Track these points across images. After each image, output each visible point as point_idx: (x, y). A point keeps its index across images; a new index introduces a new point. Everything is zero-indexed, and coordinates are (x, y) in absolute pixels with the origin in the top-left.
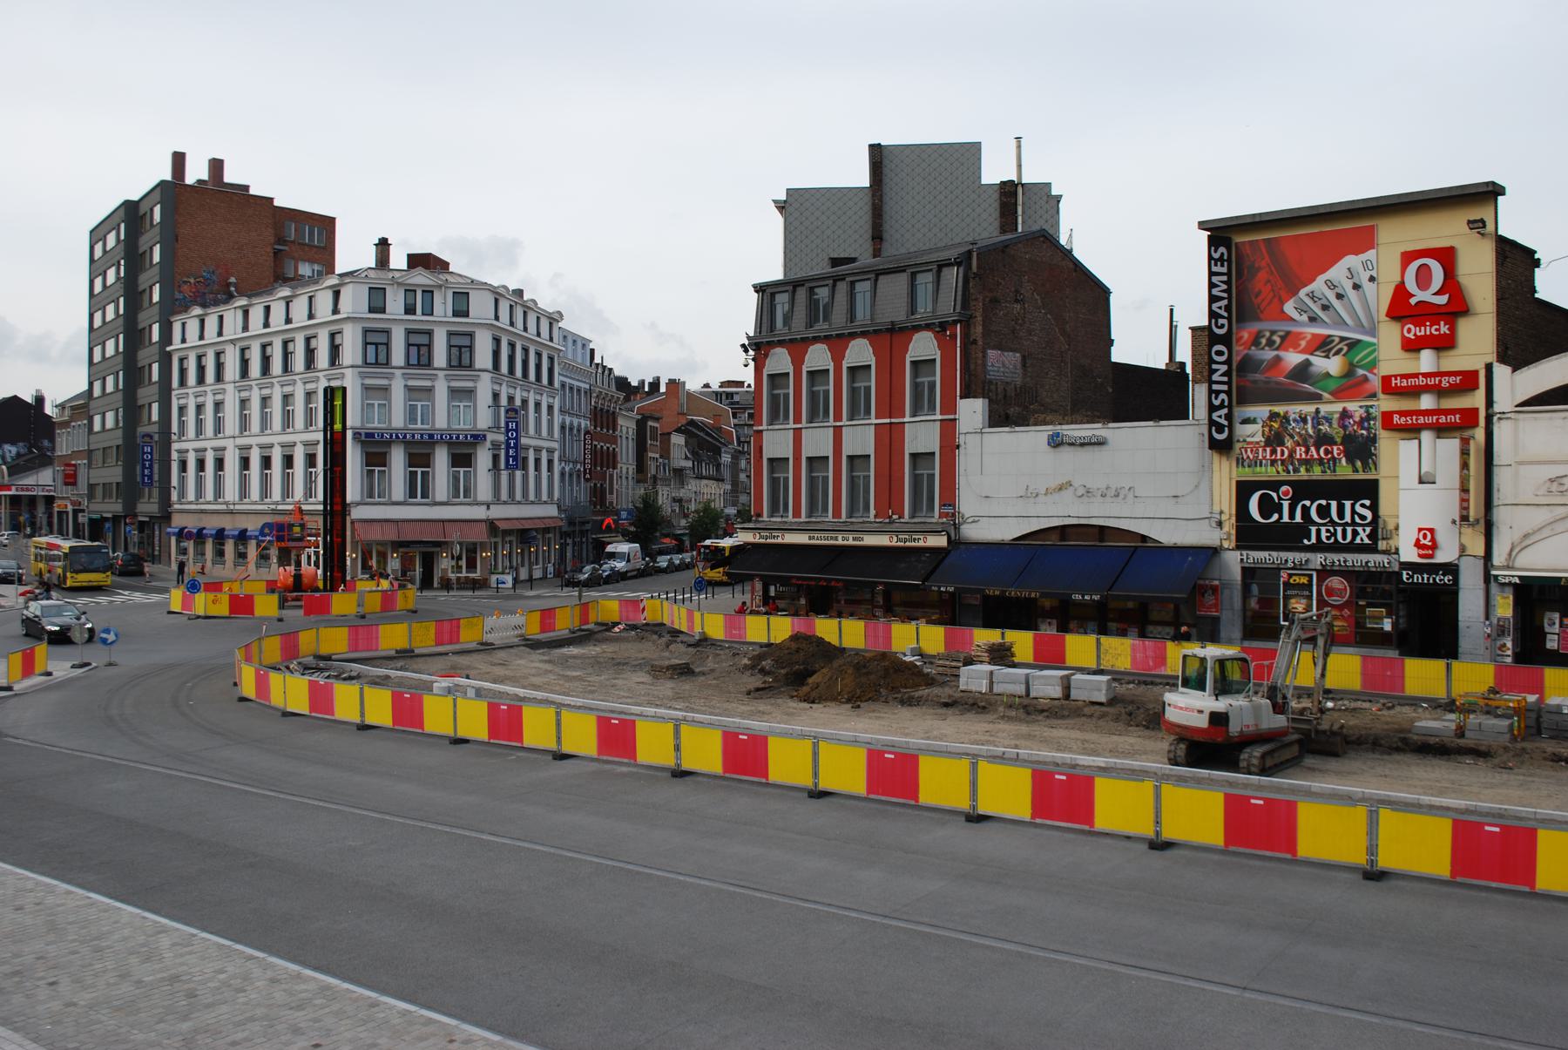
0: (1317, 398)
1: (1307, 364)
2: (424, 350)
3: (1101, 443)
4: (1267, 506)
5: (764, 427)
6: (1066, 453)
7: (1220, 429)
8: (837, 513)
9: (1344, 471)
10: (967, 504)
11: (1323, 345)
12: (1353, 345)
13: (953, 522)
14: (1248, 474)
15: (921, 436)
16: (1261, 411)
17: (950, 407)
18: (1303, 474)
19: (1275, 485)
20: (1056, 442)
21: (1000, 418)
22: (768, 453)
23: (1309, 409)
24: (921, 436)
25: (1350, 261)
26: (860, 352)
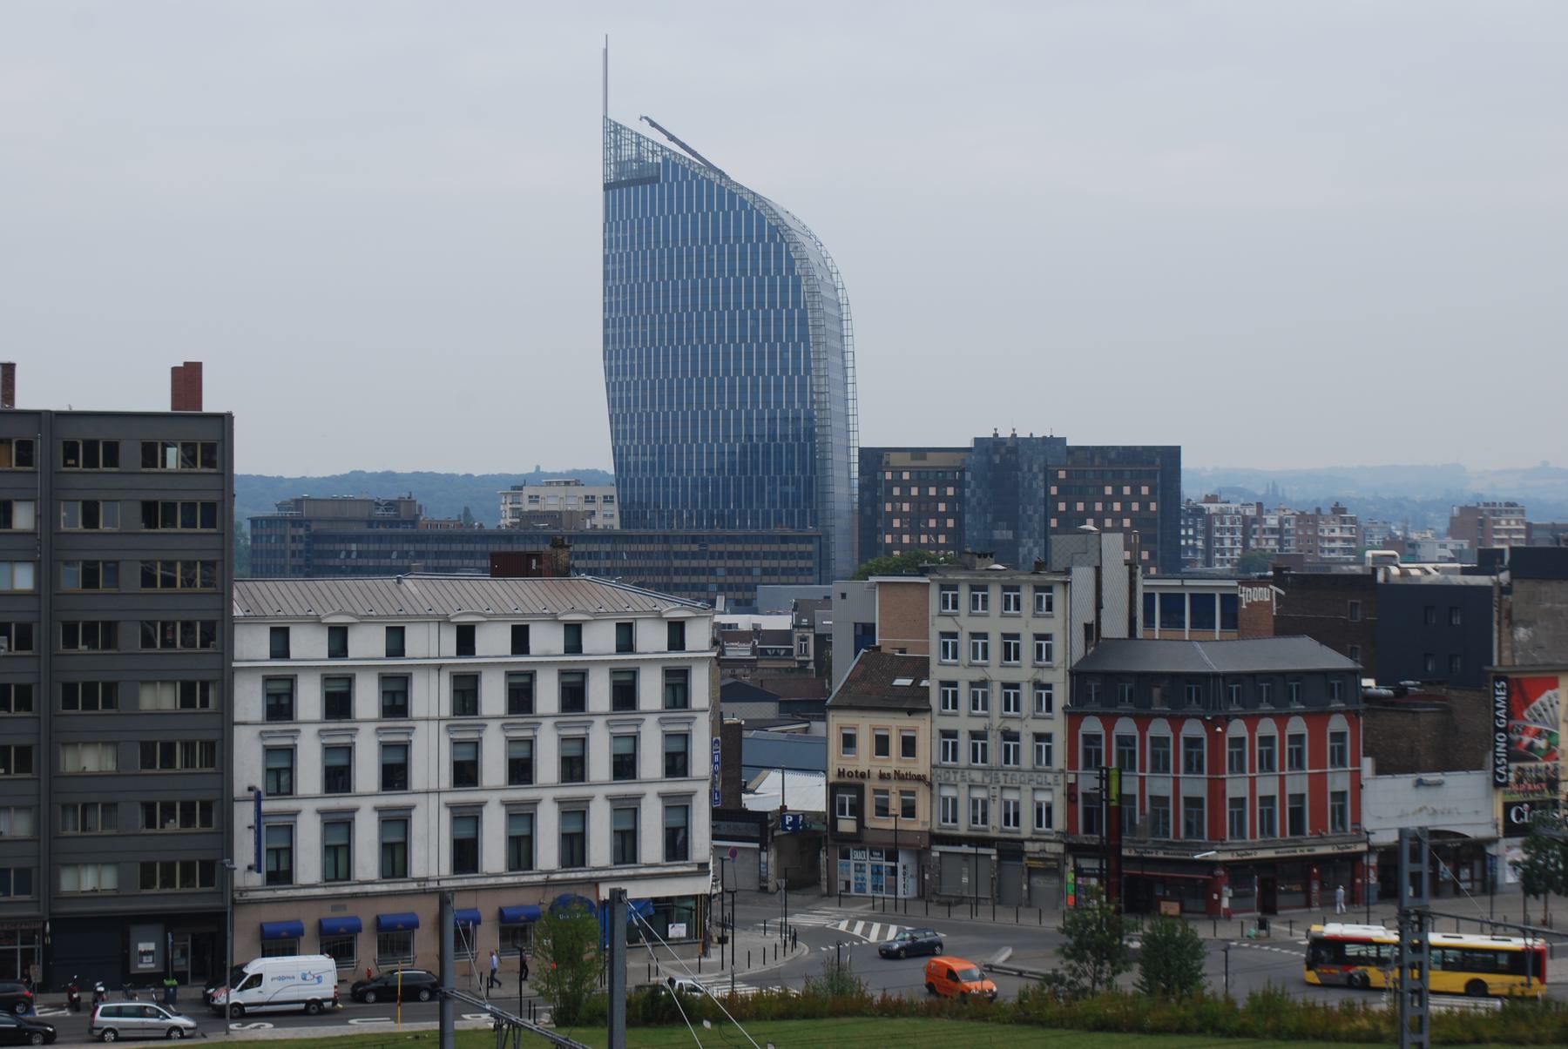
0: (1535, 760)
1: (1532, 743)
2: (679, 691)
3: (1439, 784)
4: (1520, 815)
5: (1227, 775)
6: (1423, 791)
7: (1501, 776)
8: (1253, 835)
9: (1547, 795)
10: (1368, 823)
11: (1539, 734)
12: (1550, 734)
13: (1360, 834)
14: (1509, 799)
15: (1338, 781)
16: (1513, 766)
17: (1356, 762)
18: (1531, 798)
19: (1521, 804)
20: (1419, 783)
21: (1380, 770)
22: (1230, 794)
23: (1533, 765)
24: (1338, 781)
25: (1549, 693)
26: (1297, 726)
